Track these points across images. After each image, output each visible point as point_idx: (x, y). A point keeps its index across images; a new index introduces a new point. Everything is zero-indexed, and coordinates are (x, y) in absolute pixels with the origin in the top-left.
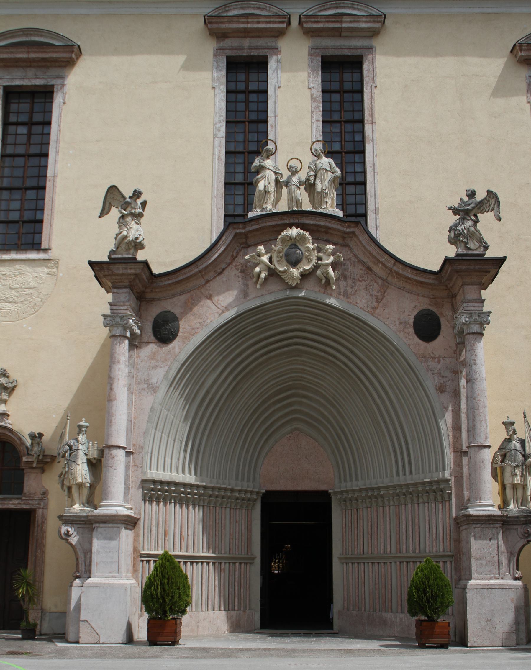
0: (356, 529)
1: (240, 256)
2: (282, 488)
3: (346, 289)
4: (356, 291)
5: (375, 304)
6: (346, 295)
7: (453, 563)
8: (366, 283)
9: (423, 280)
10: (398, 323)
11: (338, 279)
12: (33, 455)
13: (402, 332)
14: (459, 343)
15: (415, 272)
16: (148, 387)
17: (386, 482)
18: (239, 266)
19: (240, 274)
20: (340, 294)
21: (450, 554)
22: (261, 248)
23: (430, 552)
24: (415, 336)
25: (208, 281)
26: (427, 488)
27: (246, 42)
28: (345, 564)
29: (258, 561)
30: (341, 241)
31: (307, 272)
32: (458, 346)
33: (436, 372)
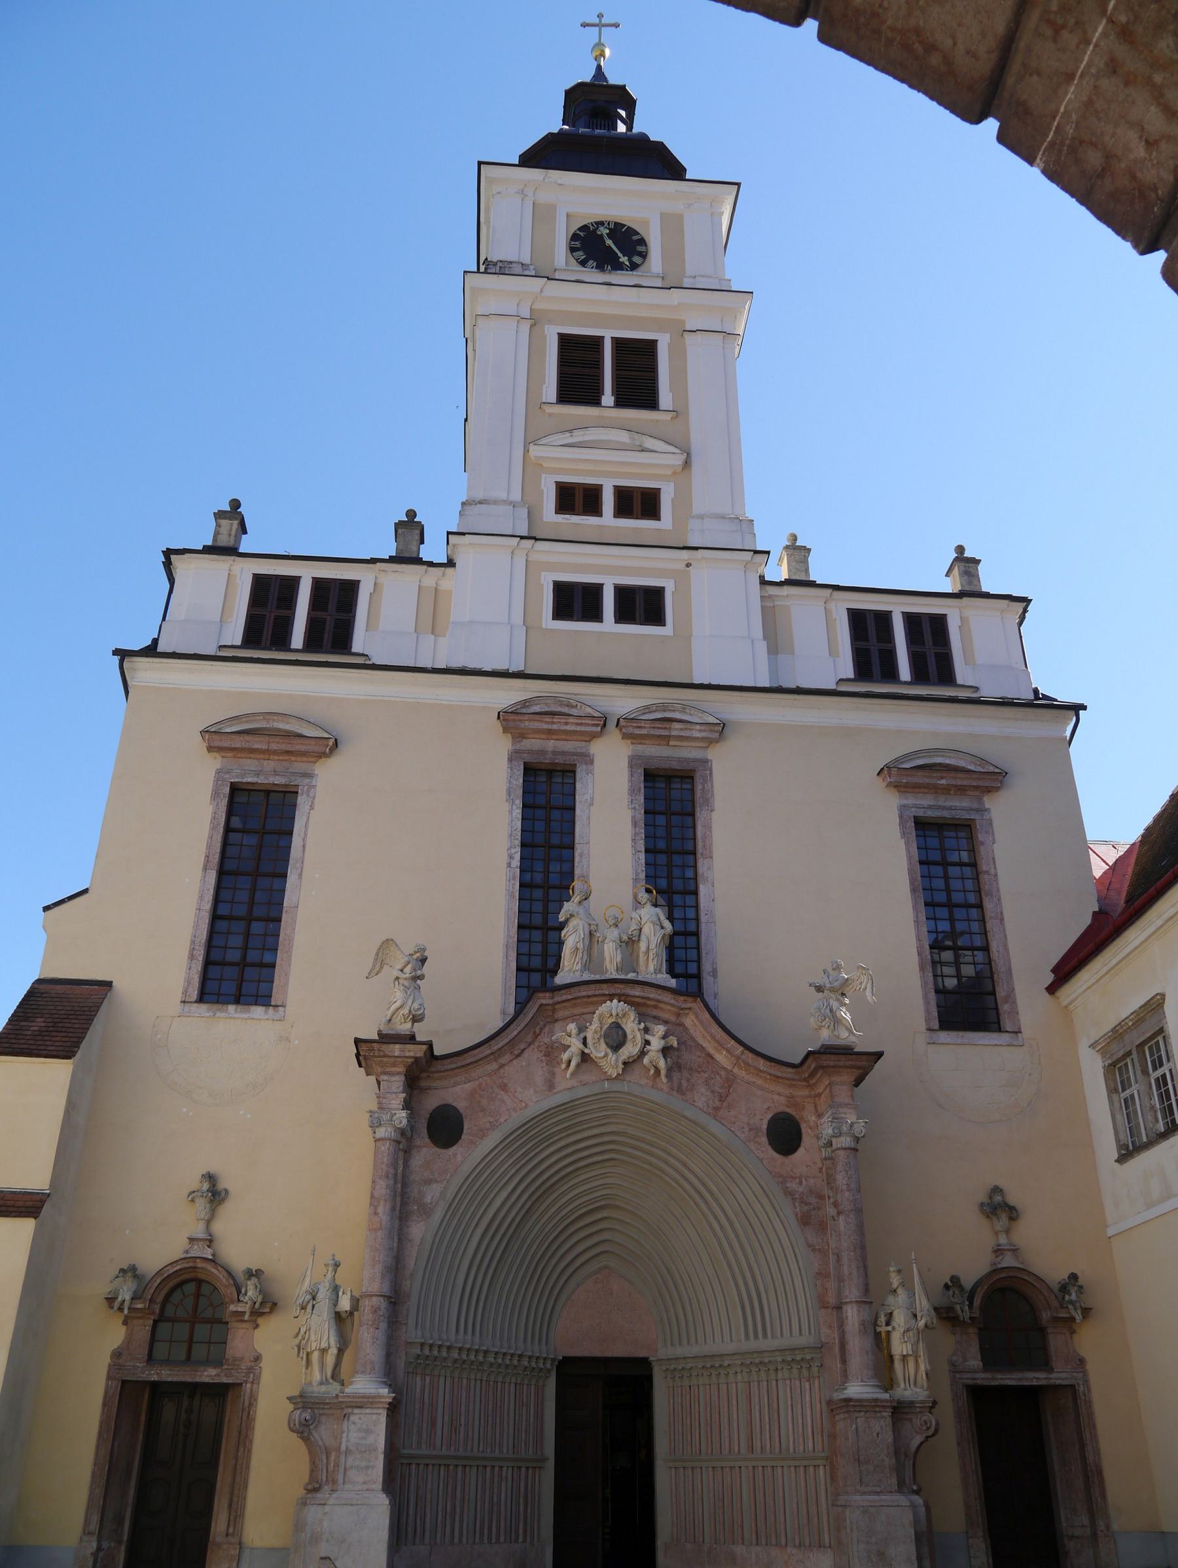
0: (689, 1416)
2: (586, 1354)
4: (693, 1085)
5: (717, 1103)
6: (680, 1090)
7: (827, 1467)
8: (706, 1075)
9: (779, 1074)
10: (746, 1129)
11: (669, 1070)
12: (247, 1303)
13: (752, 1143)
14: (826, 1159)
15: (768, 1063)
16: (418, 1209)
17: (731, 1347)
19: (544, 1058)
20: (672, 1089)
21: (823, 1454)
22: (572, 1027)
23: (795, 1452)
24: (769, 1147)
25: (502, 1066)
26: (789, 1359)
27: (551, 745)
28: (673, 1469)
29: (551, 1465)
30: (673, 1018)
31: (631, 1060)
32: (824, 1162)
33: (797, 1196)
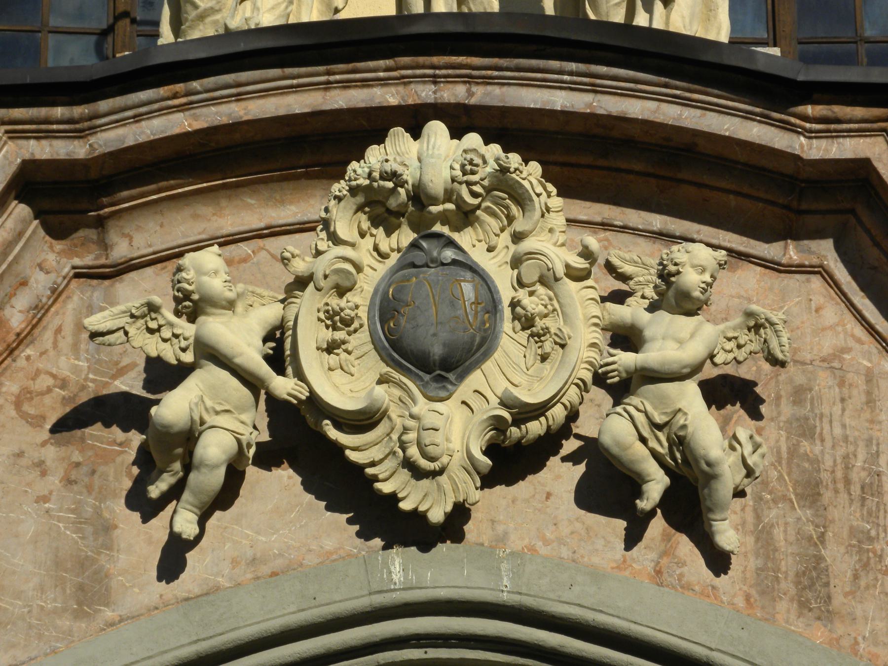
1: (59, 330)
3: (819, 559)
18: (47, 400)
19: (51, 453)
